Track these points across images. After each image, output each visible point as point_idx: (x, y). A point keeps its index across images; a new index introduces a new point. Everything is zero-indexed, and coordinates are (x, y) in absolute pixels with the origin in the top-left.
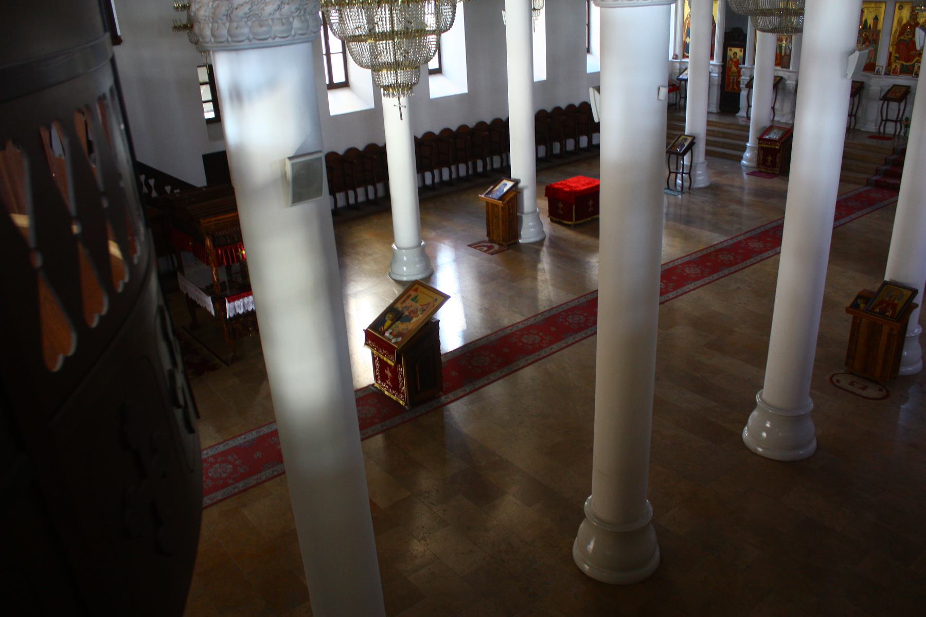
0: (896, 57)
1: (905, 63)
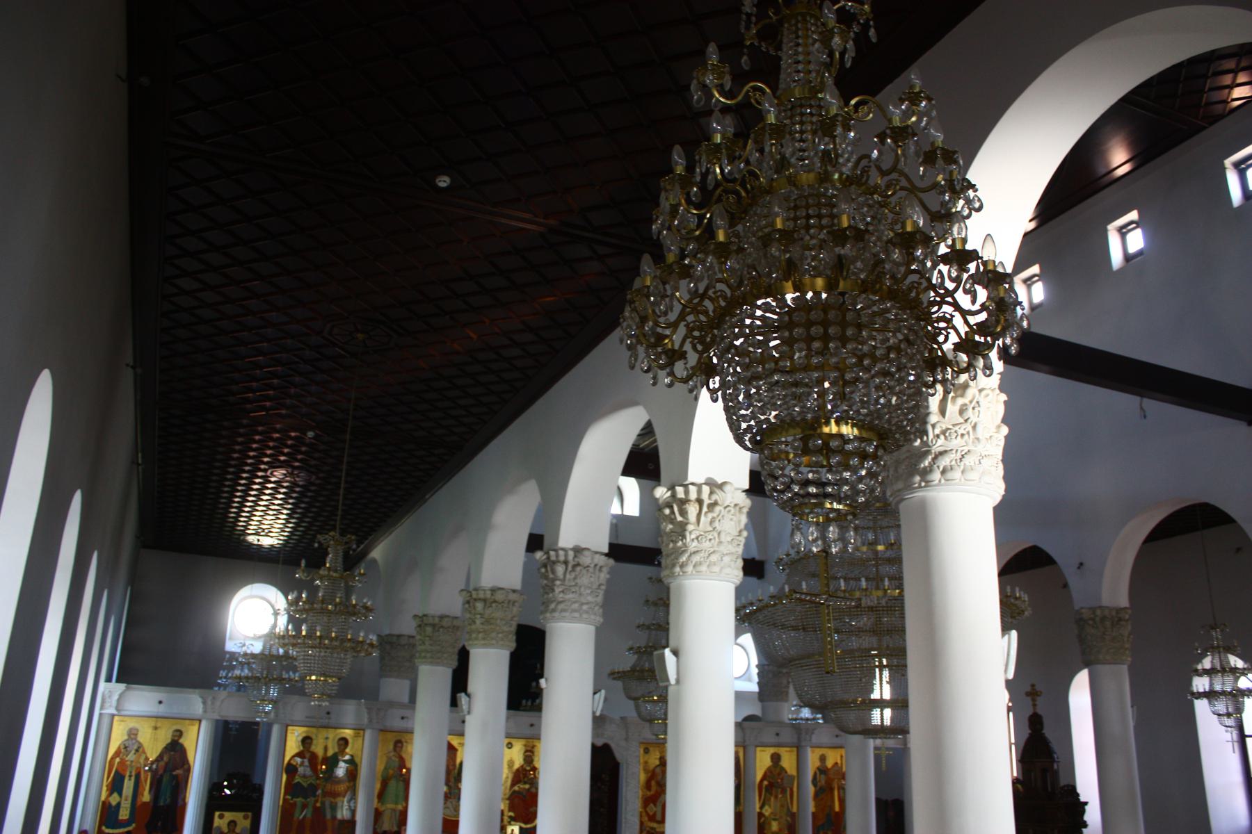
0: (510, 817)
1: (523, 826)
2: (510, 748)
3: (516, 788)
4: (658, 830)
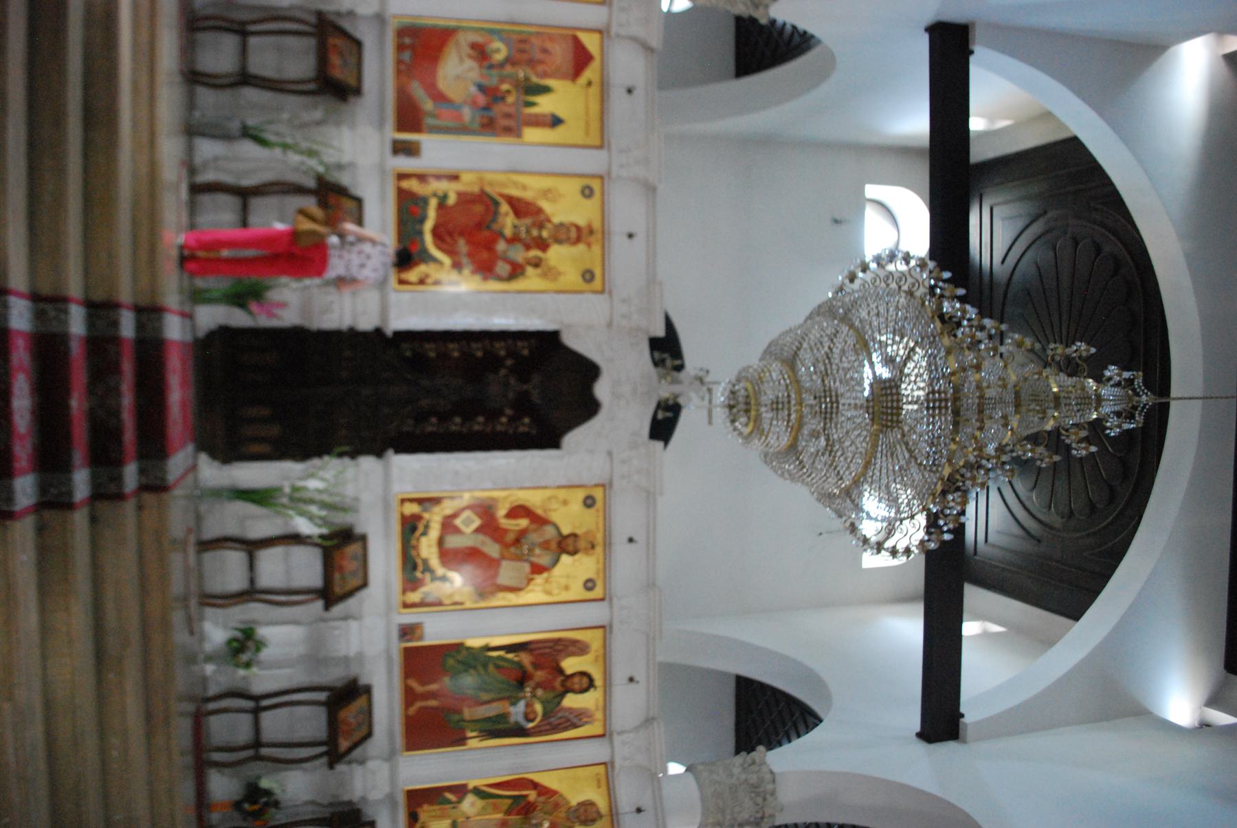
1: (429, 225)
2: (583, 193)
3: (505, 208)
4: (424, 540)
